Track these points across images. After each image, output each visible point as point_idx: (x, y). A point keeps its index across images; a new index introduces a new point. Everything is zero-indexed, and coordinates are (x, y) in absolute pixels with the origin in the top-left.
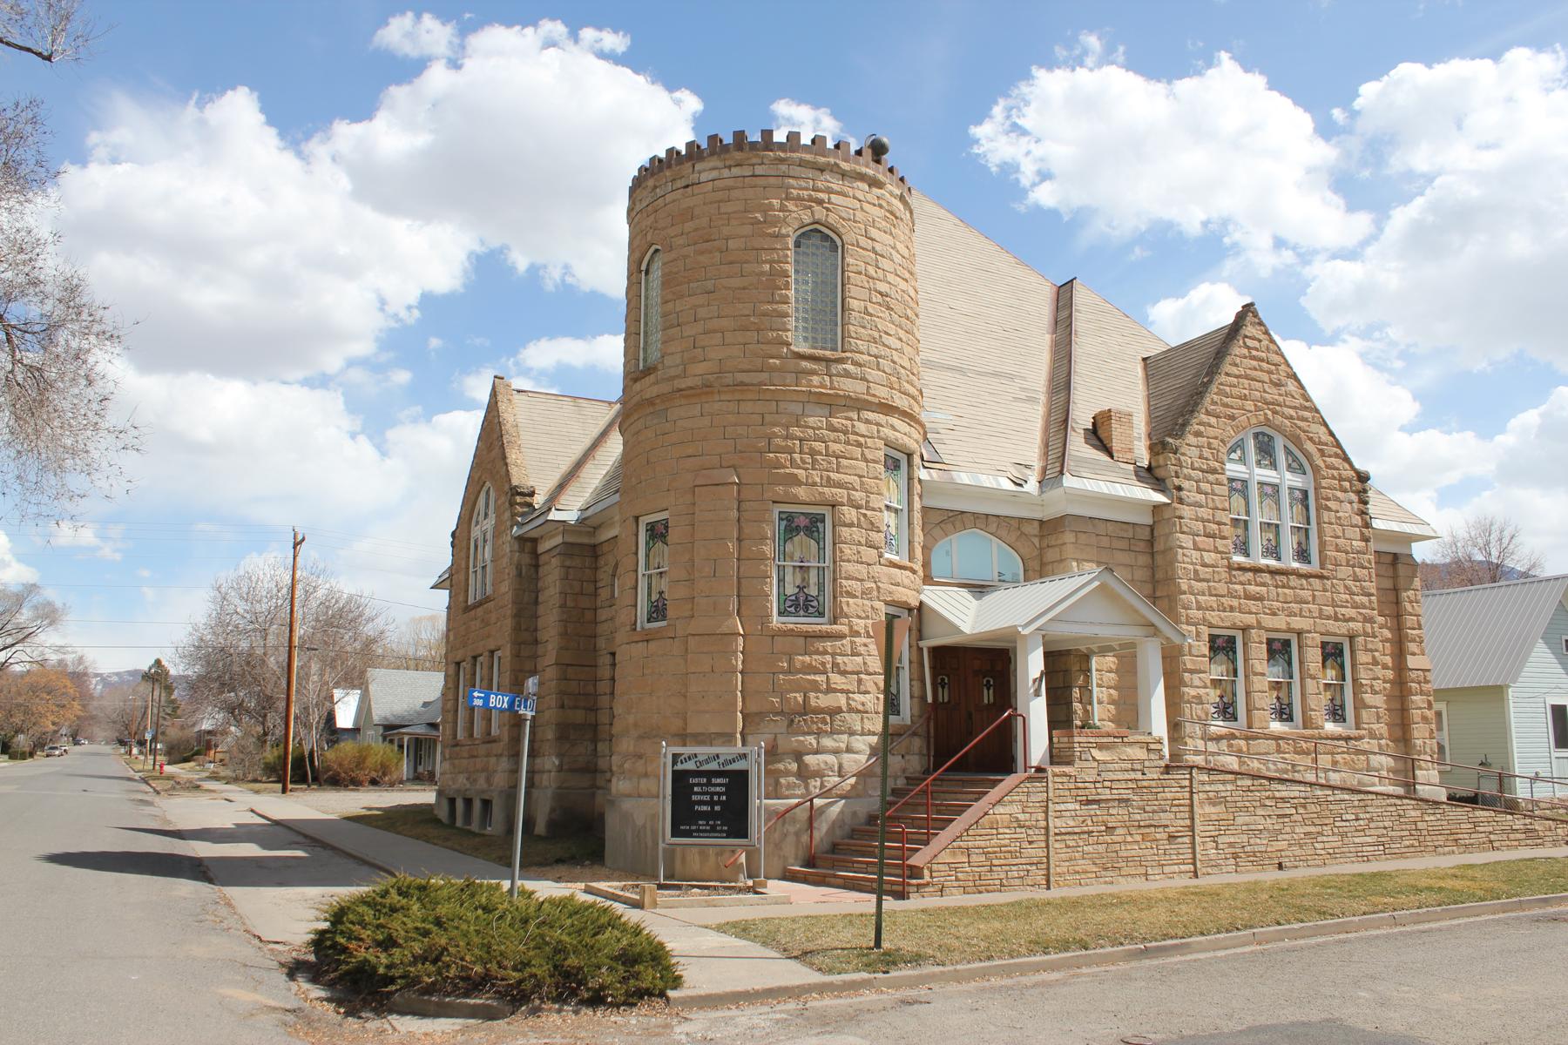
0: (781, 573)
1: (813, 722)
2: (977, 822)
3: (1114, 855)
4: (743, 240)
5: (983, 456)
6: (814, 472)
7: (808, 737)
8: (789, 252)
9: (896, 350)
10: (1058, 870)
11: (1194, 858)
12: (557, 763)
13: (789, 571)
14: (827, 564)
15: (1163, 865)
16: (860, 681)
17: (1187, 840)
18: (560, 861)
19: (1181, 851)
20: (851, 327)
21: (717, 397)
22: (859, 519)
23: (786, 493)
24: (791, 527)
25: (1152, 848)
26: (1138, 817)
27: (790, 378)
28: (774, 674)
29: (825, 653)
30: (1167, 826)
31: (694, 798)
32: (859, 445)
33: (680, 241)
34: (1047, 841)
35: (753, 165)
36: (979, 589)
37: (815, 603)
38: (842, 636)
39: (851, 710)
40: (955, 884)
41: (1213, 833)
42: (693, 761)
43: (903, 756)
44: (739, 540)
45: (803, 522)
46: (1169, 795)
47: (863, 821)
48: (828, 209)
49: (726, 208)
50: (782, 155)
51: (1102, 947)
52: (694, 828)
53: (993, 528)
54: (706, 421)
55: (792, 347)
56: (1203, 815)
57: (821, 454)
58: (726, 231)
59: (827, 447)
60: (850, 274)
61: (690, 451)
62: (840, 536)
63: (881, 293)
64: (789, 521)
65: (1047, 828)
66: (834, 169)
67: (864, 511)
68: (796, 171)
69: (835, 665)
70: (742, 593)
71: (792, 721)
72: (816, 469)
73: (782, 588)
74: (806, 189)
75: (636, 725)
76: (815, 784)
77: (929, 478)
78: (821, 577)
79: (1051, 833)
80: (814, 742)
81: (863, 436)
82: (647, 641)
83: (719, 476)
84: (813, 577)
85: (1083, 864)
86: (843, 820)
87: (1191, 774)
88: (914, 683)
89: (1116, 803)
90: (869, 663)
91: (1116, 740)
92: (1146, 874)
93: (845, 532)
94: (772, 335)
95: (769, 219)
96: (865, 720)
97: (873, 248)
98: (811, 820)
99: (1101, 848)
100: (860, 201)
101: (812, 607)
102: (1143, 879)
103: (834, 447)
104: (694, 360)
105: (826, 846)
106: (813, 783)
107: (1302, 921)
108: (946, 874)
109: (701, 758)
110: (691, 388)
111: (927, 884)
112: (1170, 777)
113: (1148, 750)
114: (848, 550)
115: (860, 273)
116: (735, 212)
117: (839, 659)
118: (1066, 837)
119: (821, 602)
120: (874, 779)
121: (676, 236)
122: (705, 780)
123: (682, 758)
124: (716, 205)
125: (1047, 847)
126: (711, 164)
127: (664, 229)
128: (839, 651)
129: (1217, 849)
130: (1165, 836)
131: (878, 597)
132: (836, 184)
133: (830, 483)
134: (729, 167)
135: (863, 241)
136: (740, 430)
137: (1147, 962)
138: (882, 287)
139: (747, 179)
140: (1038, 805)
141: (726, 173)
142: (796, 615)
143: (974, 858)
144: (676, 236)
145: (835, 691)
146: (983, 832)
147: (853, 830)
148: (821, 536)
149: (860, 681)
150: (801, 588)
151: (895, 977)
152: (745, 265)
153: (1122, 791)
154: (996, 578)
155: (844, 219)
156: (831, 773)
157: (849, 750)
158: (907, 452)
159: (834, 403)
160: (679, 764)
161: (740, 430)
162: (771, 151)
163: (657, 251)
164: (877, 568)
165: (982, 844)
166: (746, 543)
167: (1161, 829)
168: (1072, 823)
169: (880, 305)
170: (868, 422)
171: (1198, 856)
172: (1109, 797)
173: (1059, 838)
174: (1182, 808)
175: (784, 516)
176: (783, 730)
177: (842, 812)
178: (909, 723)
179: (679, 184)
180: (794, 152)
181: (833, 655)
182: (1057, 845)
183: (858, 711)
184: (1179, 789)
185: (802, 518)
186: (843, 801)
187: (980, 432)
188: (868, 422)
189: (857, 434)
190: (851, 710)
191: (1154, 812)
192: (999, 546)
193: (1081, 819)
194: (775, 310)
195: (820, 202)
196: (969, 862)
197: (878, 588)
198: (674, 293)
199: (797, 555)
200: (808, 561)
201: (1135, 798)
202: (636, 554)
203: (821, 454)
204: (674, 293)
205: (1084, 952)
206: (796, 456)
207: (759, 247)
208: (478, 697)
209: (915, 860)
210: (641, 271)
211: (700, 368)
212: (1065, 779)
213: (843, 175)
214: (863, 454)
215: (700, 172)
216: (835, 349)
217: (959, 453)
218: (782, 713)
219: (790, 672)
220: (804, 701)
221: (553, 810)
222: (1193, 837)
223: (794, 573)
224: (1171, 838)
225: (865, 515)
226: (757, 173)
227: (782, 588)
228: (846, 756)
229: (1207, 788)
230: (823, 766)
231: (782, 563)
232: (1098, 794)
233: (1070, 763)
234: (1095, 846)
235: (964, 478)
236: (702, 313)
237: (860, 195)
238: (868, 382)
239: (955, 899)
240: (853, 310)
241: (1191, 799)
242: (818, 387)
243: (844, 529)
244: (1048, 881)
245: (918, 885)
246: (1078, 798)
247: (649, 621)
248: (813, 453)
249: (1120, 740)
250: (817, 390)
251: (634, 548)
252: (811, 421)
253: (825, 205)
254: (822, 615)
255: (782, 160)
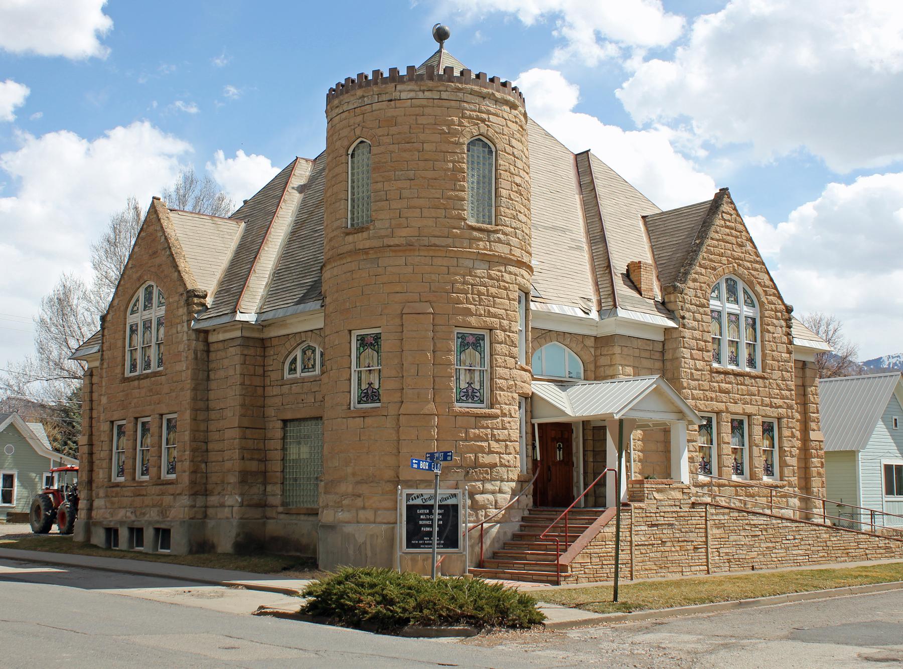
0: (458, 374)
1: (481, 473)
2: (595, 537)
3: (665, 559)
4: (434, 144)
5: (562, 292)
6: (480, 307)
7: (477, 483)
8: (465, 155)
9: (524, 223)
10: (637, 568)
11: (707, 562)
12: (239, 500)
13: (462, 372)
14: (486, 368)
15: (691, 566)
16: (506, 446)
17: (703, 550)
18: (285, 569)
19: (700, 557)
20: (502, 209)
21: (417, 253)
22: (505, 339)
23: (464, 321)
24: (464, 345)
25: (685, 555)
26: (678, 535)
27: (466, 243)
28: (456, 441)
29: (487, 427)
30: (693, 541)
31: (421, 522)
32: (506, 289)
33: (388, 140)
34: (631, 550)
35: (440, 91)
36: (562, 384)
37: (478, 394)
38: (496, 417)
39: (502, 465)
40: (584, 576)
41: (717, 546)
42: (420, 499)
43: (527, 496)
44: (434, 352)
45: (471, 339)
46: (694, 522)
47: (509, 538)
48: (488, 126)
49: (421, 120)
50: (460, 86)
51: (720, 602)
52: (421, 542)
53: (567, 341)
54: (410, 269)
55: (468, 222)
56: (712, 535)
57: (484, 295)
58: (422, 137)
59: (488, 290)
60: (502, 172)
61: (398, 289)
62: (495, 350)
63: (517, 185)
64: (462, 339)
65: (631, 542)
66: (492, 97)
67: (508, 333)
68: (469, 98)
69: (493, 435)
70: (436, 387)
71: (468, 472)
72: (481, 305)
73: (458, 384)
74: (475, 111)
75: (354, 474)
76: (482, 513)
77: (536, 309)
78: (482, 376)
79: (633, 545)
80: (481, 486)
81: (508, 283)
82: (364, 417)
83: (420, 307)
84: (477, 378)
85: (650, 565)
86: (499, 538)
87: (706, 508)
88: (528, 447)
89: (666, 527)
90: (512, 435)
91: (666, 487)
92: (682, 572)
93: (498, 347)
94: (455, 212)
95: (452, 131)
96: (509, 472)
97: (513, 153)
98: (481, 536)
99: (659, 554)
100: (506, 119)
101: (477, 397)
102: (681, 574)
103: (493, 290)
104: (399, 226)
105: (490, 554)
106: (481, 513)
107: (807, 591)
108: (579, 569)
109: (425, 497)
110: (398, 246)
111: (569, 576)
112: (695, 510)
113: (683, 493)
114: (500, 360)
115: (506, 171)
116: (428, 124)
117: (496, 432)
118: (641, 547)
119: (482, 394)
120: (514, 511)
121: (383, 135)
122: (428, 511)
123: (413, 496)
124: (414, 117)
125: (631, 553)
126: (410, 87)
127: (372, 129)
128: (495, 426)
129: (719, 556)
130: (692, 547)
131: (515, 391)
132: (492, 108)
133: (490, 315)
134: (423, 91)
135: (508, 149)
136: (433, 277)
137: (741, 610)
138: (518, 180)
139: (435, 101)
140: (626, 527)
141: (421, 95)
142: (466, 402)
143: (594, 560)
144: (383, 135)
145: (493, 452)
146: (598, 543)
147: (505, 544)
148: (482, 349)
149: (506, 446)
150: (470, 384)
151: (635, 615)
152: (435, 162)
153: (670, 519)
154: (567, 375)
155: (497, 133)
156: (491, 507)
157: (500, 491)
158: (526, 291)
159: (492, 261)
160: (411, 500)
161: (433, 277)
162: (453, 82)
163: (362, 142)
164: (515, 371)
165: (598, 551)
166: (438, 353)
167: (690, 543)
168: (643, 539)
169: (517, 193)
170: (510, 273)
171: (710, 560)
172: (663, 522)
173: (637, 548)
174: (701, 530)
175: (460, 336)
176: (462, 478)
177: (498, 532)
178: (526, 473)
179: (385, 97)
180: (467, 84)
181: (492, 429)
182: (636, 553)
183: (506, 466)
184: (699, 518)
185: (471, 337)
186: (499, 525)
187: (557, 274)
188: (510, 273)
189: (504, 281)
190: (502, 465)
191: (686, 532)
192: (569, 354)
193: (648, 536)
194: (457, 196)
195: (483, 121)
196: (591, 562)
197: (516, 384)
198: (383, 177)
199: (468, 363)
200: (475, 366)
201: (676, 523)
202: (350, 356)
203: (484, 295)
204: (383, 177)
205: (712, 604)
206: (469, 295)
207: (445, 150)
208: (415, 463)
209: (563, 560)
210: (348, 155)
211: (404, 232)
212: (640, 511)
213: (496, 101)
214: (507, 295)
215: (400, 92)
216: (490, 223)
217: (549, 290)
218: (461, 467)
219: (466, 440)
220: (475, 459)
221: (238, 535)
222: (707, 548)
223: (465, 374)
224: (696, 548)
225: (509, 336)
226: (443, 97)
227: (458, 384)
228: (499, 495)
229: (715, 517)
230: (486, 502)
231: (457, 367)
232: (657, 520)
233: (641, 501)
234: (656, 553)
235: (556, 309)
236: (406, 193)
237: (506, 116)
238: (511, 246)
239: (584, 584)
240: (503, 197)
241: (706, 524)
242: (483, 250)
243: (498, 345)
244: (632, 575)
245: (565, 577)
246: (647, 523)
247: (359, 402)
248: (480, 294)
249: (668, 486)
250: (482, 252)
251: (349, 352)
252: (479, 272)
253: (487, 123)
254: (482, 402)
255: (459, 90)
